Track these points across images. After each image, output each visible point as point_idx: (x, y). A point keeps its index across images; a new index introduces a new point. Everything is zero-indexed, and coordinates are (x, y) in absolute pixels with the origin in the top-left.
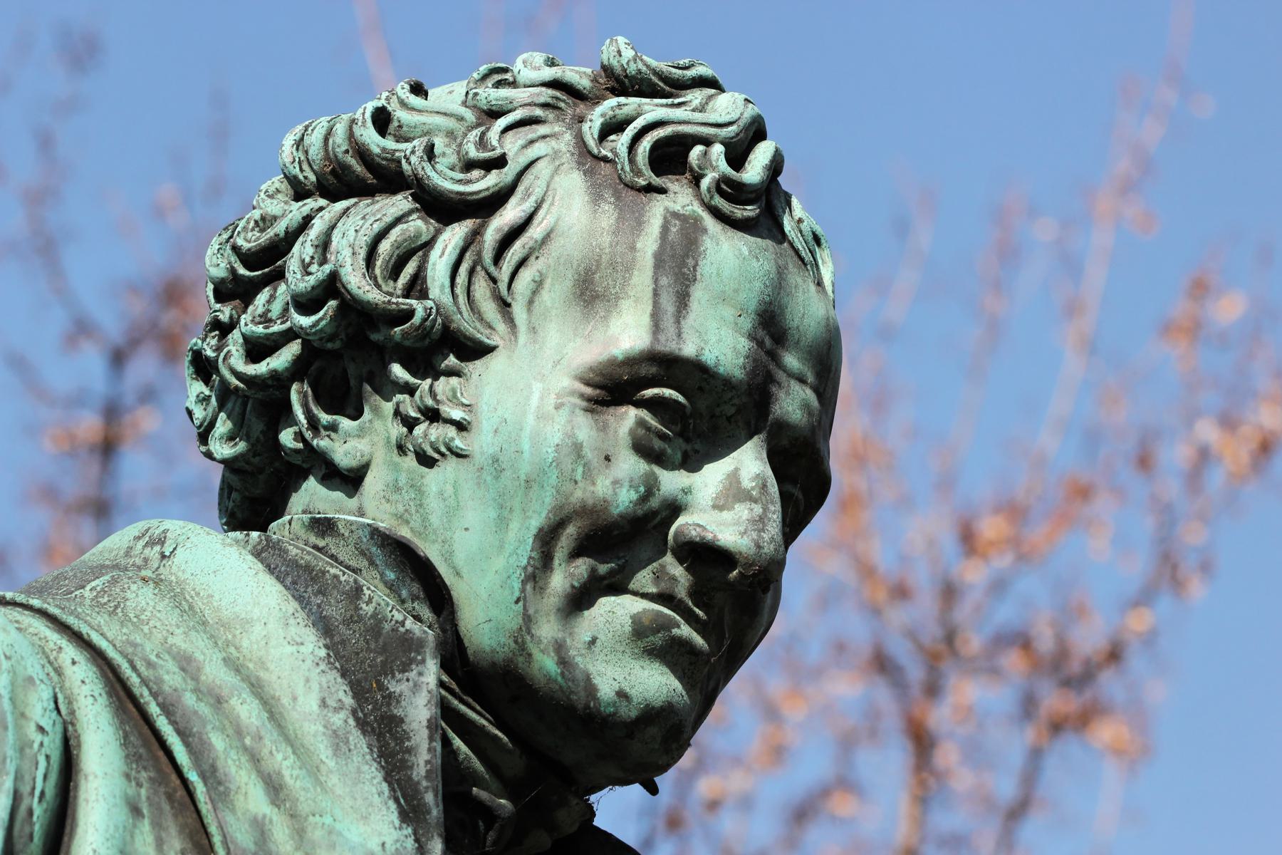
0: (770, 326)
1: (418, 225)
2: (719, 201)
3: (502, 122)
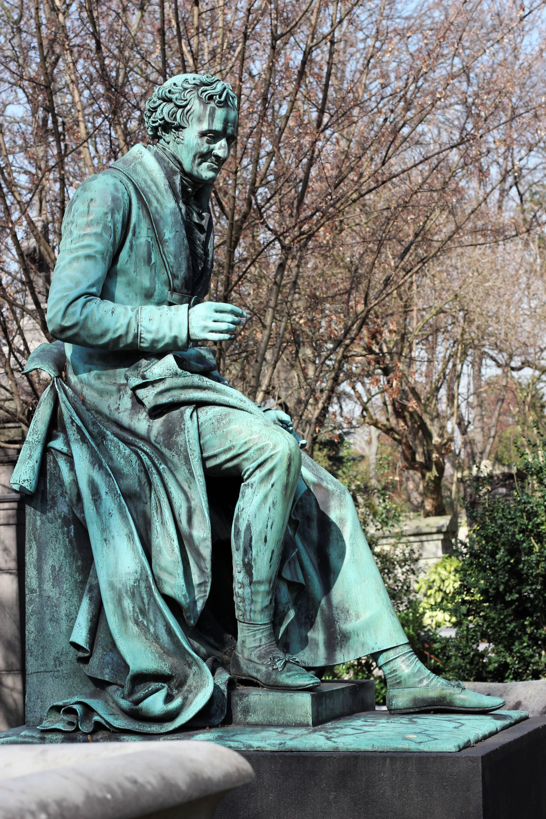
0: (226, 121)
1: (175, 109)
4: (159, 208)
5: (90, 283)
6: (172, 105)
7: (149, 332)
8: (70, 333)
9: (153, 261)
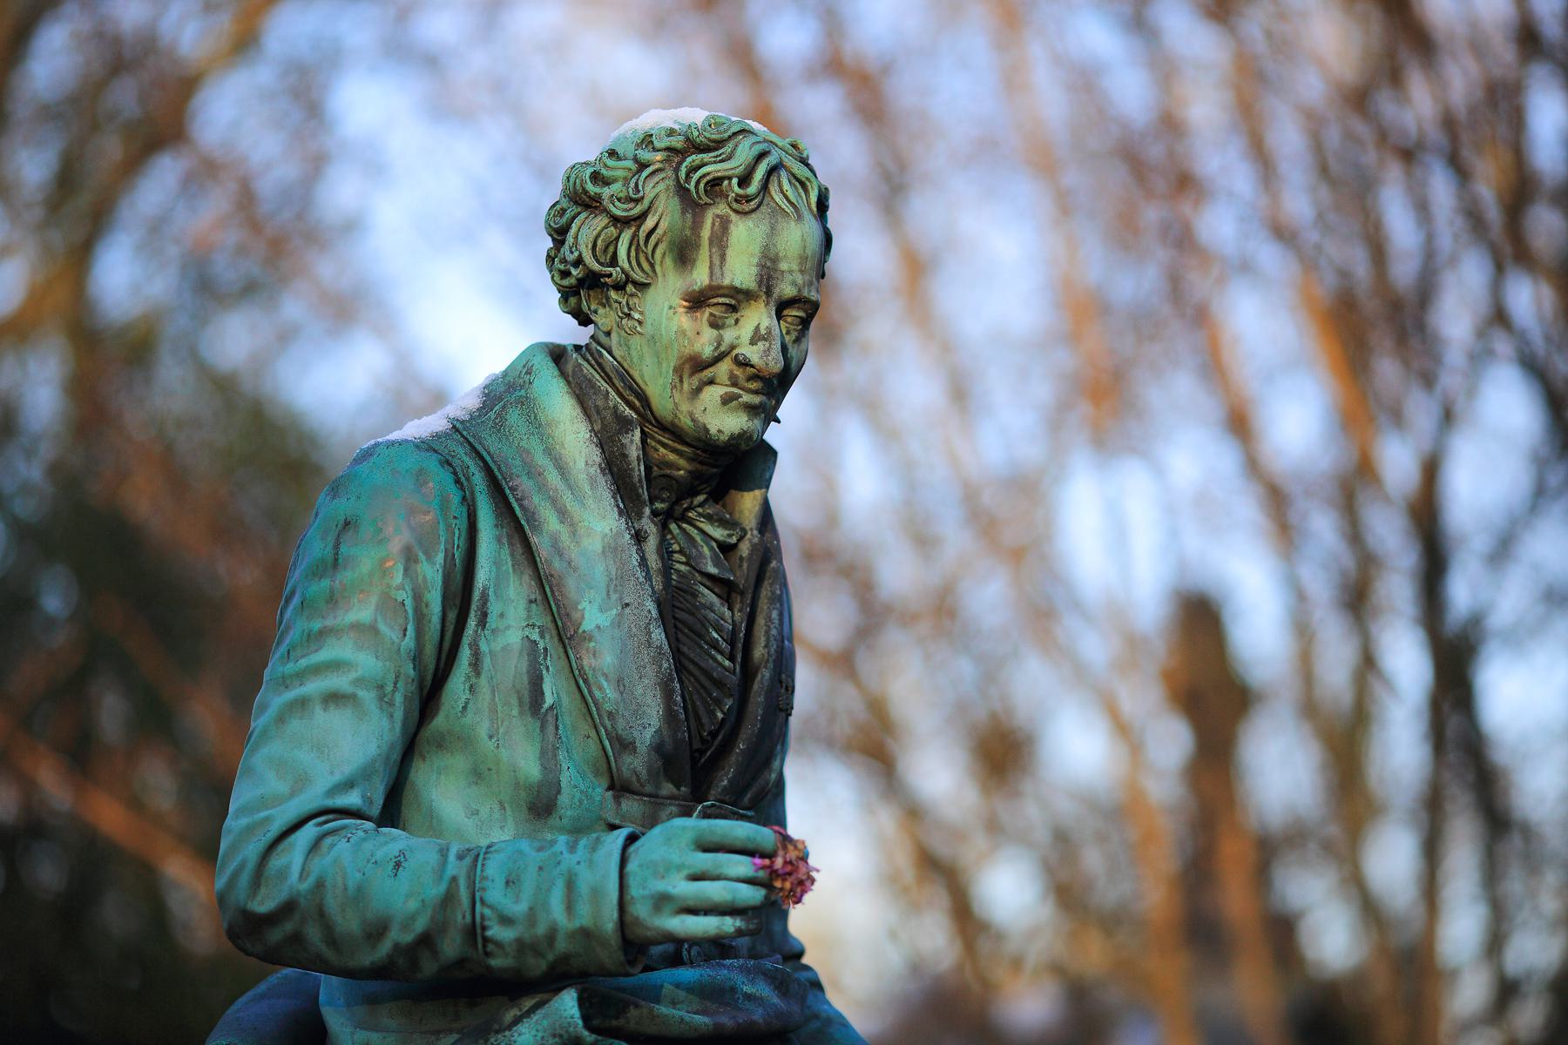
2: (735, 206)
3: (645, 174)
4: (565, 538)
5: (337, 778)
6: (600, 221)
7: (506, 921)
8: (276, 935)
9: (549, 700)
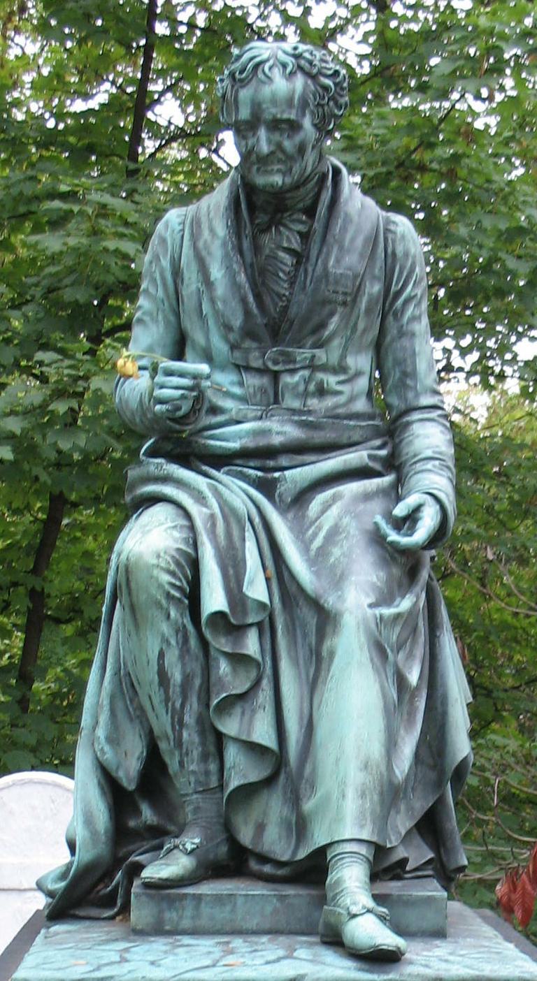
9: (204, 313)
